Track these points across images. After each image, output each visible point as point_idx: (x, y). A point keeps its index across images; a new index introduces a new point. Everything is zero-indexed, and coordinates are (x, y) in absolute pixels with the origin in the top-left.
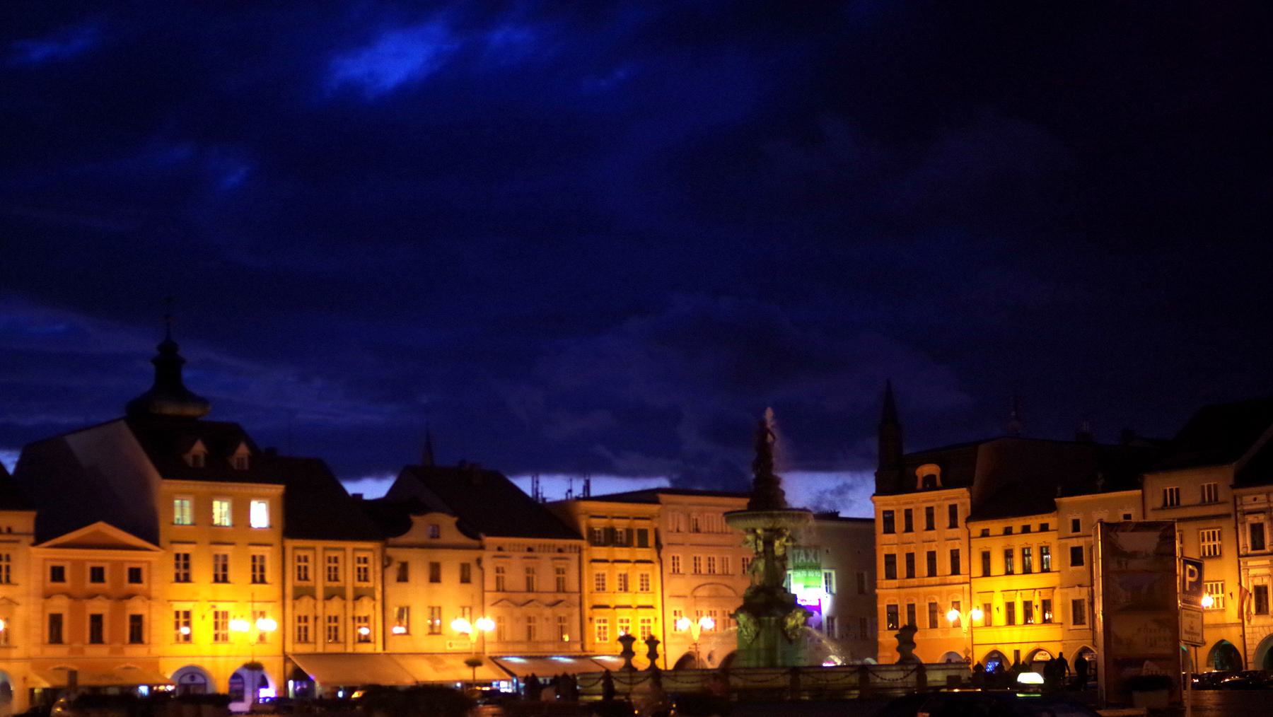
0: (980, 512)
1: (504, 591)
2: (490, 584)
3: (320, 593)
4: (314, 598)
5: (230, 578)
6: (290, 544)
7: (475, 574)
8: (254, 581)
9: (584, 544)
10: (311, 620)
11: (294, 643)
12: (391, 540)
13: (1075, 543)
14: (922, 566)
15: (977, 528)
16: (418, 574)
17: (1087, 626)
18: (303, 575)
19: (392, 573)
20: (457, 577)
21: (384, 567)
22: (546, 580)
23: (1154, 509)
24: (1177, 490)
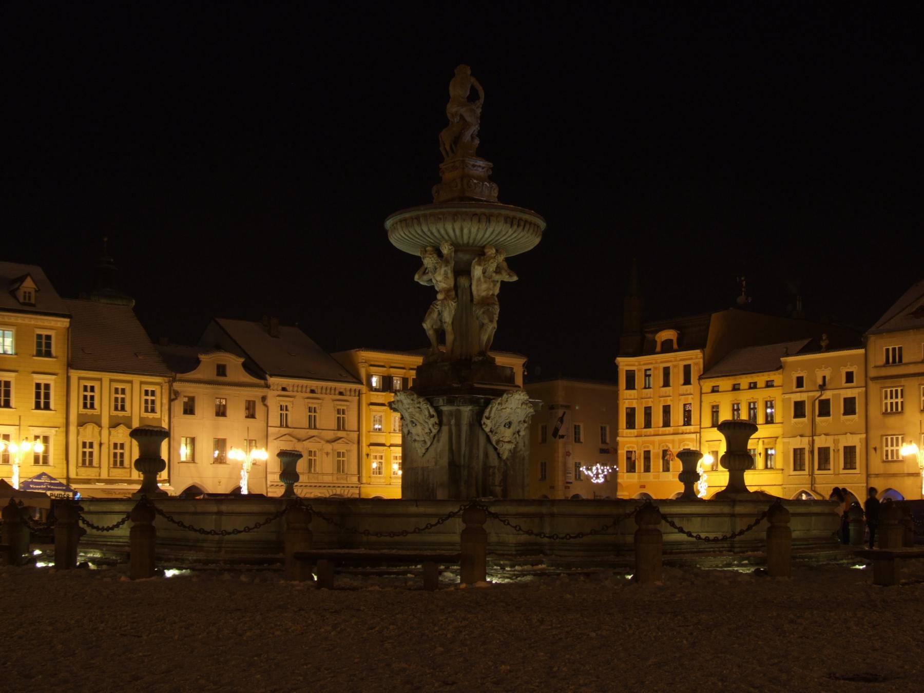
0: (709, 371)
1: (287, 426)
2: (274, 420)
3: (105, 421)
4: (100, 426)
5: (13, 403)
6: (75, 374)
7: (260, 410)
8: (38, 406)
9: (364, 388)
10: (96, 446)
11: (77, 467)
12: (179, 376)
13: (798, 397)
14: (658, 417)
15: (708, 385)
16: (205, 410)
17: (806, 472)
18: (89, 403)
19: (178, 407)
20: (243, 413)
21: (171, 400)
22: (327, 419)
23: (876, 367)
24: (900, 349)
